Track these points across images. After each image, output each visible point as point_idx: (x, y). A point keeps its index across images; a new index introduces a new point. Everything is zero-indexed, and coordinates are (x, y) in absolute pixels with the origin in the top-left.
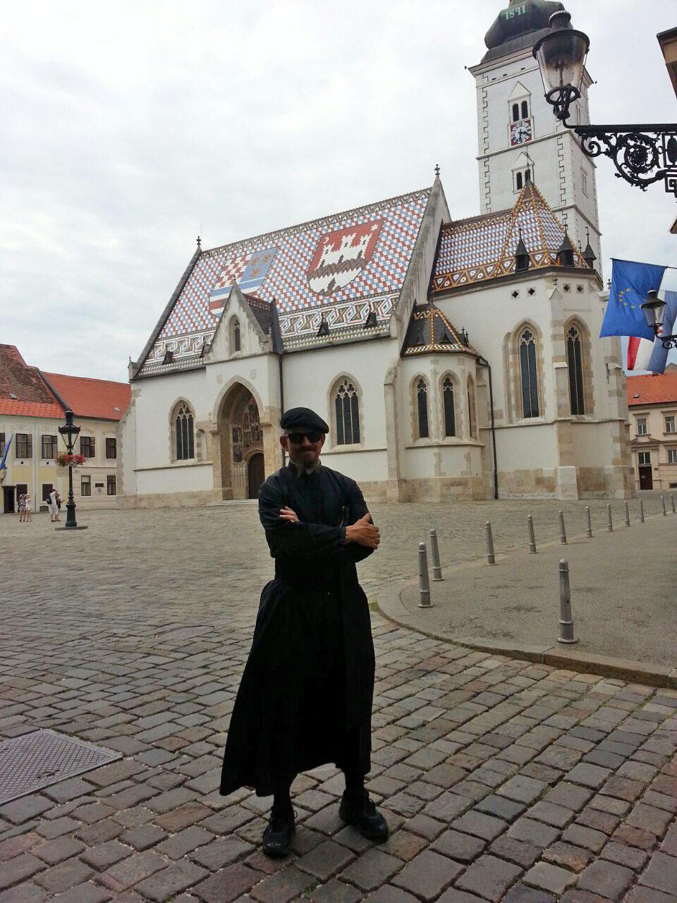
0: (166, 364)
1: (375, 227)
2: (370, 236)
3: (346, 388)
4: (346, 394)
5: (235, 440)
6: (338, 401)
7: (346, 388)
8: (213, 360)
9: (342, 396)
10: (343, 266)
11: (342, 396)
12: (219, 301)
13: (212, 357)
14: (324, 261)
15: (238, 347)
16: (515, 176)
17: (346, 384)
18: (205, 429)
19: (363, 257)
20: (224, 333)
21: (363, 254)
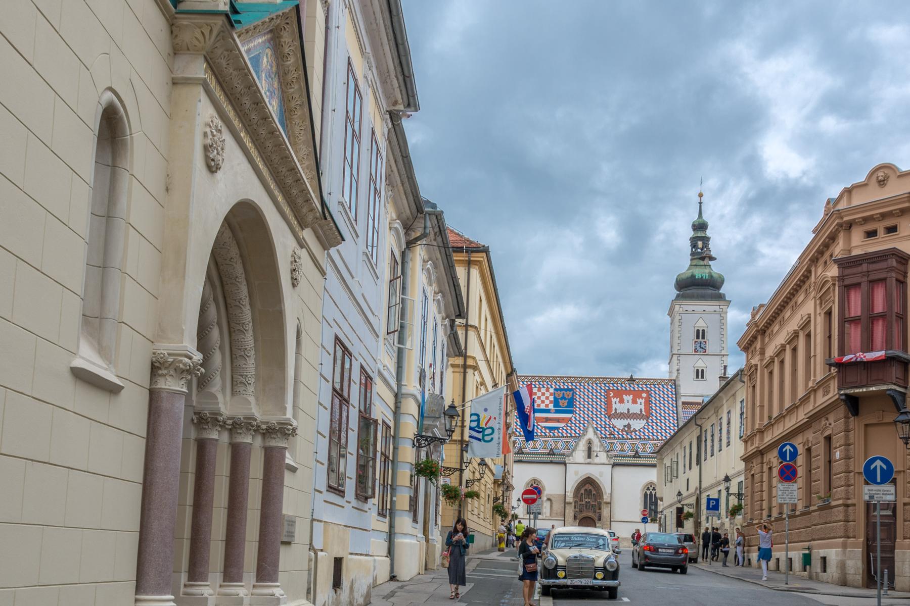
0: (520, 454)
1: (644, 395)
2: (644, 400)
3: (651, 488)
4: (651, 492)
5: (575, 507)
6: (646, 495)
7: (651, 488)
8: (572, 461)
9: (648, 492)
10: (628, 415)
11: (648, 492)
12: (543, 418)
13: (571, 460)
14: (616, 409)
15: (589, 456)
16: (695, 371)
17: (651, 486)
18: (553, 499)
19: (643, 413)
20: (582, 445)
21: (643, 411)
